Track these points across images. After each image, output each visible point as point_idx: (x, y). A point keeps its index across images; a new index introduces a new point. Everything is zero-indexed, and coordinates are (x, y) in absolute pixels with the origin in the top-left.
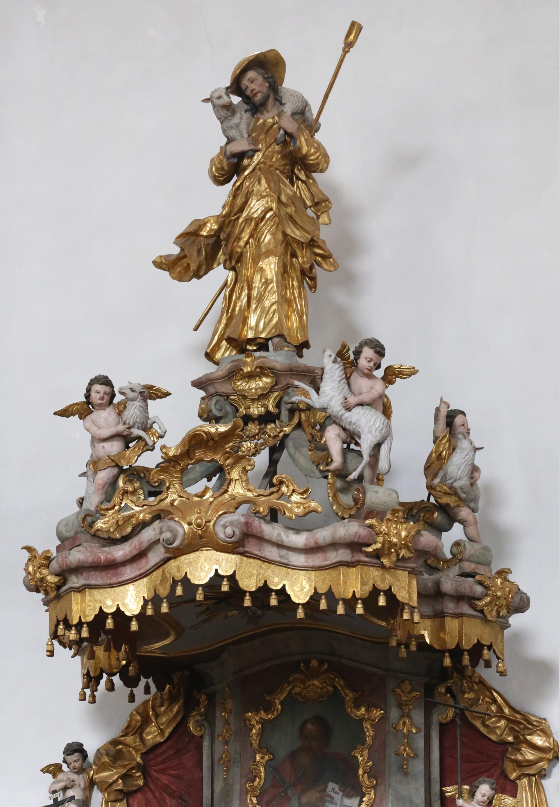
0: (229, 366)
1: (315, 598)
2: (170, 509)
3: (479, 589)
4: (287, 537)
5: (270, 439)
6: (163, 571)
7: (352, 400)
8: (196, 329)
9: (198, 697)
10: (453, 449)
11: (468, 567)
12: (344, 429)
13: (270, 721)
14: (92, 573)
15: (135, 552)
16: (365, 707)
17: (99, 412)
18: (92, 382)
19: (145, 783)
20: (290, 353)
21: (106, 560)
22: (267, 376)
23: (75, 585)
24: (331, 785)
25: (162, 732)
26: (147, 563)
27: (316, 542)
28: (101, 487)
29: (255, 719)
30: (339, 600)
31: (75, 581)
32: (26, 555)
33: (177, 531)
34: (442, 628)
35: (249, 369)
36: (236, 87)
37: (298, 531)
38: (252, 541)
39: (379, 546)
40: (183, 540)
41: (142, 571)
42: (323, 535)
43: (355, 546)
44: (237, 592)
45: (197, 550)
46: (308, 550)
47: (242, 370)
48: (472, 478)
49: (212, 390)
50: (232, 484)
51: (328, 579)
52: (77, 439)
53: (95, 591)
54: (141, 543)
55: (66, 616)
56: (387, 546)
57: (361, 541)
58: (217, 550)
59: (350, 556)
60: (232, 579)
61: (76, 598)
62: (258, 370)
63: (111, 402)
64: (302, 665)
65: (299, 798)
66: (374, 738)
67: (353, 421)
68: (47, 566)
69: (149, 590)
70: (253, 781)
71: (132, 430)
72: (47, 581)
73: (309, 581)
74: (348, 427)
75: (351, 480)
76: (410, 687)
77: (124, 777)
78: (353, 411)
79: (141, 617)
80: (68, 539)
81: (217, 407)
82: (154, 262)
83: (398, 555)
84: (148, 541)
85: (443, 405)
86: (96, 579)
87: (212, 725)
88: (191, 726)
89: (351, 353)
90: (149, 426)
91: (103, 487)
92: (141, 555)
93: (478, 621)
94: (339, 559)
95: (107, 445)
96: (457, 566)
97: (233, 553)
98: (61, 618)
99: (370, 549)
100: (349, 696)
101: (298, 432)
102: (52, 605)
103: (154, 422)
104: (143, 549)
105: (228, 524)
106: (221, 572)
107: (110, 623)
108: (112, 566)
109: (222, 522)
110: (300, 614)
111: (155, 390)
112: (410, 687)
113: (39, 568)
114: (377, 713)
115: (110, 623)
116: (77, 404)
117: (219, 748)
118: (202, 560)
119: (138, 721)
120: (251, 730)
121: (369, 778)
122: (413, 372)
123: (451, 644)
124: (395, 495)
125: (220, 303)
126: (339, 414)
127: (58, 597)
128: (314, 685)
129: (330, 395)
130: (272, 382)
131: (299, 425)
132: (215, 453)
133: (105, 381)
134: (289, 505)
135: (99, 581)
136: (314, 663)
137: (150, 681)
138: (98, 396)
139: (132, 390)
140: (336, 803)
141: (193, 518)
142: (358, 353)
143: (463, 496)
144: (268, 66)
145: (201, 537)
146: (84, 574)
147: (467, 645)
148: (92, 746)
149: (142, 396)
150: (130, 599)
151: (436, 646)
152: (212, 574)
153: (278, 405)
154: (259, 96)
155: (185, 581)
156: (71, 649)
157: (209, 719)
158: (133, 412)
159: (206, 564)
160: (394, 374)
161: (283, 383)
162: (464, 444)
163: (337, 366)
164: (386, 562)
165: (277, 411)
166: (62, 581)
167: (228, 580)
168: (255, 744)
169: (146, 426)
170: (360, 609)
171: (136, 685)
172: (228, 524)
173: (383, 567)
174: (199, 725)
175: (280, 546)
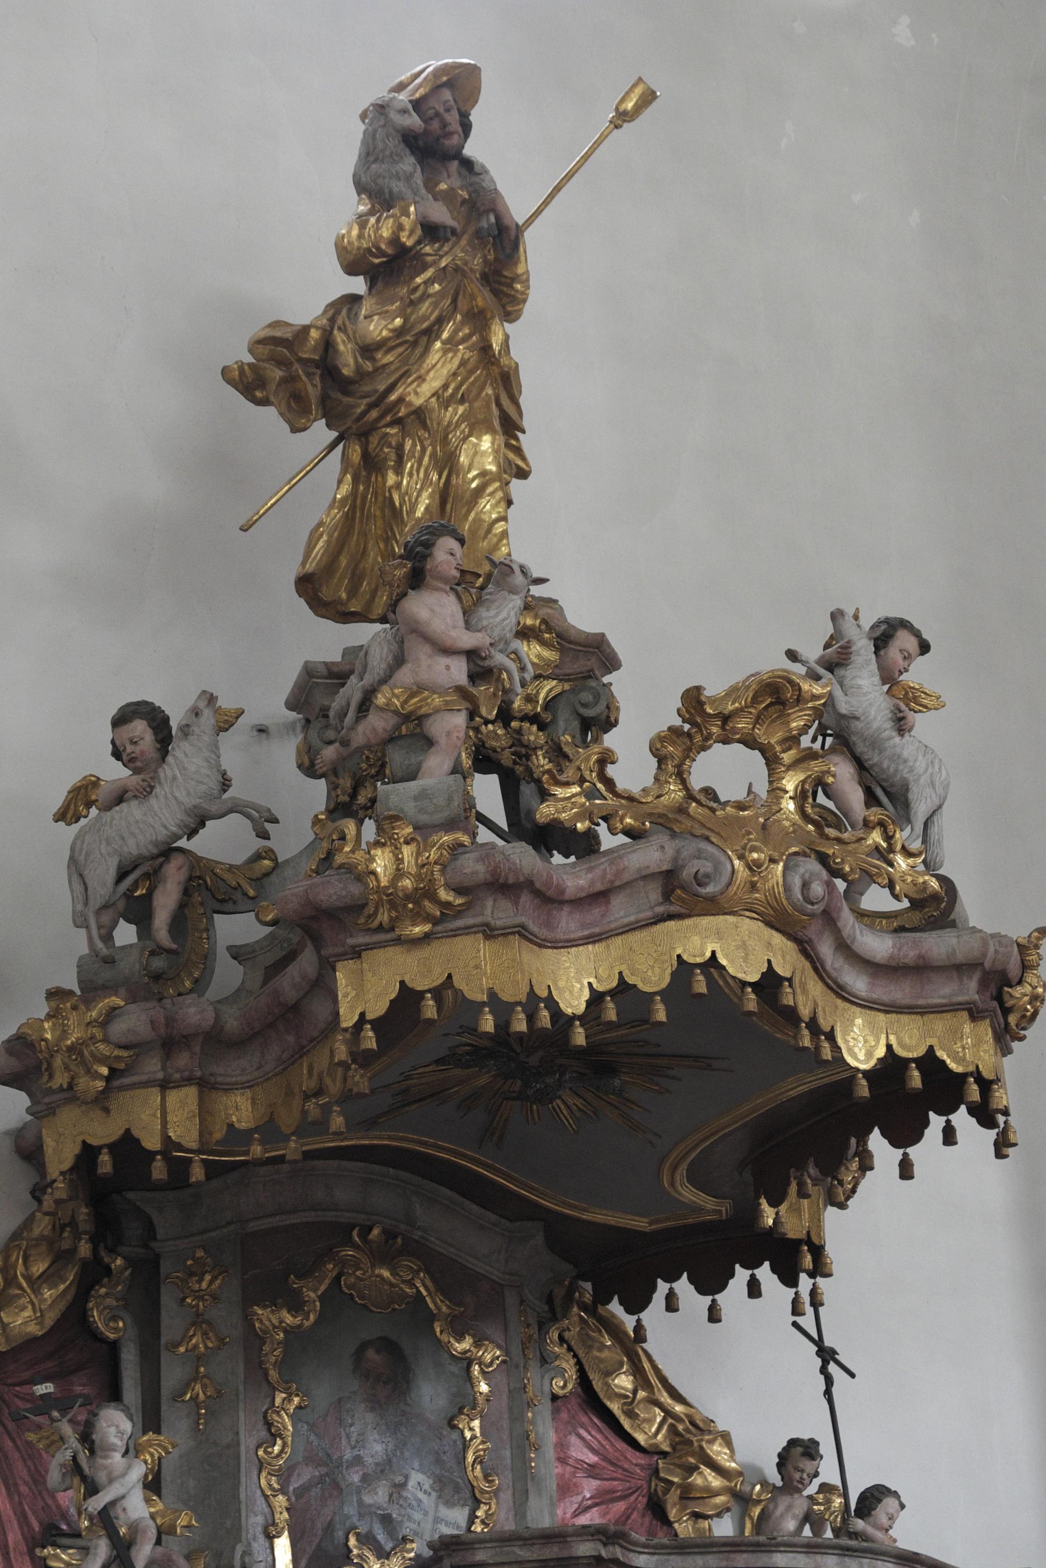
4: (862, 935)
9: (107, 1260)
16: (473, 1336)
25: (40, 1320)
26: (603, 916)
84: (639, 870)
110: (863, 1089)
168: (273, 1375)
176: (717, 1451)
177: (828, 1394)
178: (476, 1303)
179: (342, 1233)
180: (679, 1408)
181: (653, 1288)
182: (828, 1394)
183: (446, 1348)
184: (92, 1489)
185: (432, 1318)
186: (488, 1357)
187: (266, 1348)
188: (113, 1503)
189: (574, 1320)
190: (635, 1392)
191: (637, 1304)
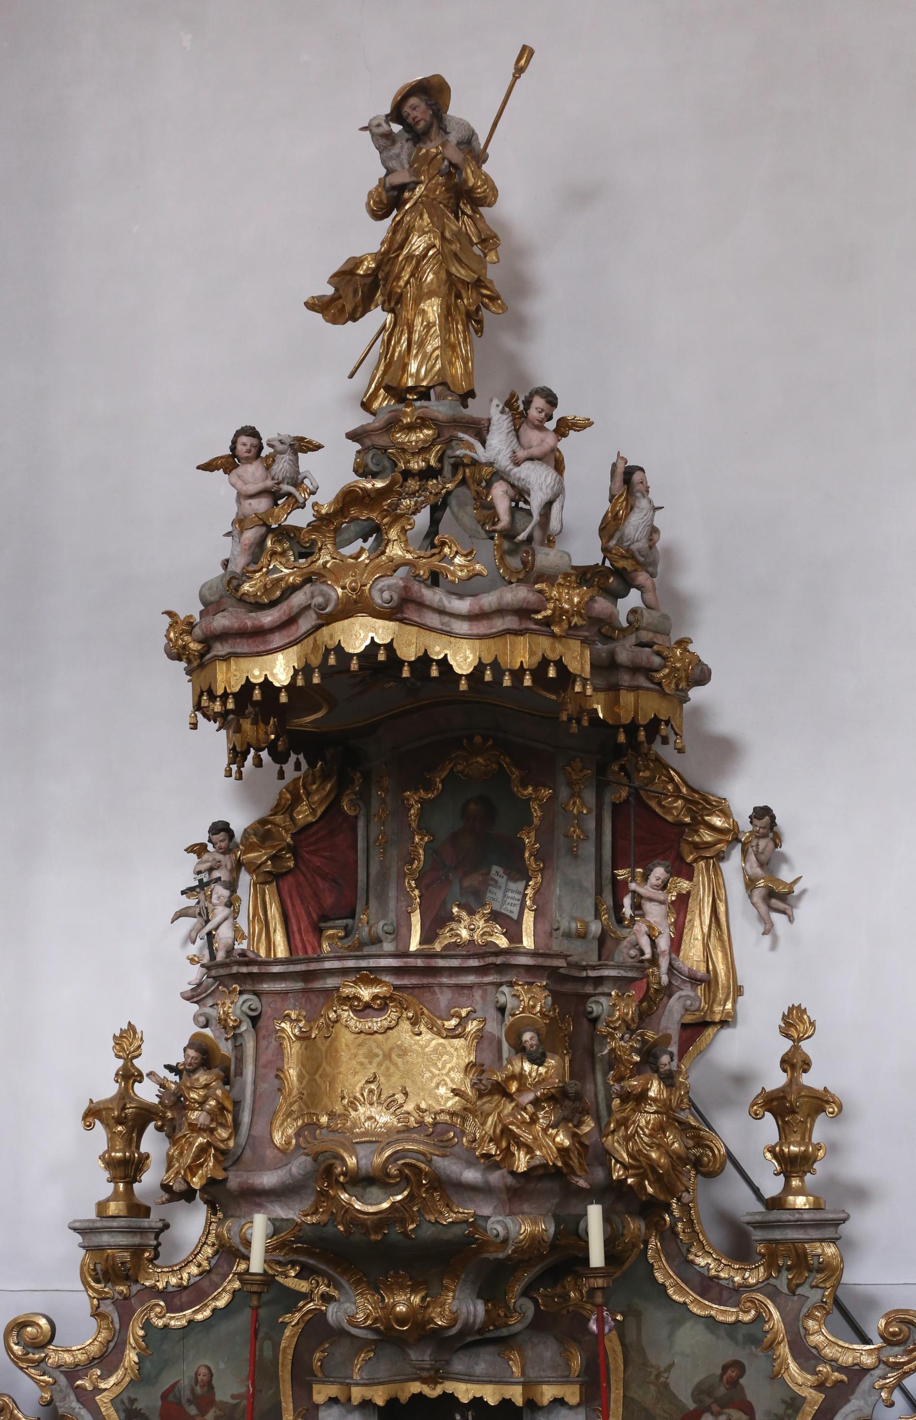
0: (387, 417)
1: (480, 668)
2: (323, 572)
3: (657, 660)
4: (450, 602)
5: (432, 496)
6: (315, 638)
7: (522, 454)
8: (351, 376)
10: (630, 508)
11: (646, 636)
12: (513, 486)
13: (429, 800)
14: (238, 640)
15: (284, 618)
16: (532, 786)
17: (245, 466)
18: (238, 434)
19: (296, 865)
20: (454, 403)
21: (253, 626)
22: (429, 428)
23: (220, 653)
24: (495, 868)
25: (314, 811)
27: (481, 609)
28: (247, 547)
29: (414, 800)
30: (505, 671)
31: (220, 649)
32: (167, 620)
33: (330, 595)
34: (616, 701)
35: (409, 420)
36: (397, 114)
37: (461, 596)
38: (412, 607)
39: (549, 612)
40: (337, 605)
41: (292, 638)
42: (489, 600)
43: (523, 612)
44: (394, 661)
45: (352, 616)
46: (471, 617)
47: (401, 421)
48: (651, 540)
49: (368, 442)
50: (390, 545)
51: (493, 648)
52: (221, 495)
53: (241, 660)
54: (291, 608)
55: (210, 687)
56: (557, 613)
57: (530, 607)
58: (373, 617)
59: (518, 624)
60: (389, 647)
61: (221, 667)
62: (419, 421)
63: (258, 455)
64: (465, 741)
65: (461, 882)
66: (542, 819)
67: (522, 477)
68: (190, 633)
69: (299, 659)
70: (412, 864)
71: (281, 486)
72: (190, 649)
73: (473, 651)
74: (516, 483)
75: (520, 540)
76: (580, 765)
77: (273, 858)
78: (523, 465)
79: (291, 687)
80: (212, 603)
81: (374, 461)
82: (306, 304)
83: (570, 623)
84: (299, 606)
85: (620, 461)
86: (243, 646)
87: (368, 805)
89: (520, 402)
90: (299, 481)
91: (250, 547)
92: (291, 621)
93: (655, 694)
94: (505, 627)
95: (254, 502)
96: (634, 636)
97: (390, 619)
98: (205, 688)
99: (539, 617)
100: (515, 774)
101: (462, 490)
102: (195, 674)
103: (305, 477)
104: (293, 615)
105: (385, 588)
106: (377, 640)
107: (257, 694)
108: (260, 633)
109: (379, 586)
110: (463, 685)
111: (307, 442)
112: (580, 765)
113: (181, 634)
114: (546, 793)
115: (257, 694)
116: (222, 457)
117: (375, 830)
118: (357, 627)
119: (288, 800)
120: (410, 810)
121: (536, 861)
122: (588, 424)
123: (626, 719)
124: (567, 558)
125: (378, 348)
126: (508, 469)
127: (202, 666)
128: (477, 762)
129: (497, 449)
130: (434, 434)
131: (463, 482)
132: (372, 510)
133: (251, 432)
134: (452, 568)
135: (246, 649)
136: (478, 739)
137: (301, 757)
138: (244, 449)
139: (281, 442)
140: (500, 887)
141: (348, 581)
142: (528, 403)
143: (642, 559)
144: (431, 92)
145: (356, 602)
146: (230, 641)
147: (642, 720)
148: (239, 825)
149: (292, 449)
150: (280, 669)
151: (610, 721)
152: (368, 642)
153: (440, 460)
154: (422, 124)
155: (339, 649)
156: (215, 722)
157: (364, 798)
158: (282, 466)
159: (361, 632)
160: (567, 426)
161: (447, 435)
162: (643, 503)
163: (505, 417)
164: (556, 630)
165: (439, 466)
166: (206, 649)
167: (385, 649)
168: (414, 825)
169: (296, 482)
170: (528, 681)
171: (286, 762)
172: (385, 588)
173: (553, 635)
174: (353, 803)
175: (442, 612)
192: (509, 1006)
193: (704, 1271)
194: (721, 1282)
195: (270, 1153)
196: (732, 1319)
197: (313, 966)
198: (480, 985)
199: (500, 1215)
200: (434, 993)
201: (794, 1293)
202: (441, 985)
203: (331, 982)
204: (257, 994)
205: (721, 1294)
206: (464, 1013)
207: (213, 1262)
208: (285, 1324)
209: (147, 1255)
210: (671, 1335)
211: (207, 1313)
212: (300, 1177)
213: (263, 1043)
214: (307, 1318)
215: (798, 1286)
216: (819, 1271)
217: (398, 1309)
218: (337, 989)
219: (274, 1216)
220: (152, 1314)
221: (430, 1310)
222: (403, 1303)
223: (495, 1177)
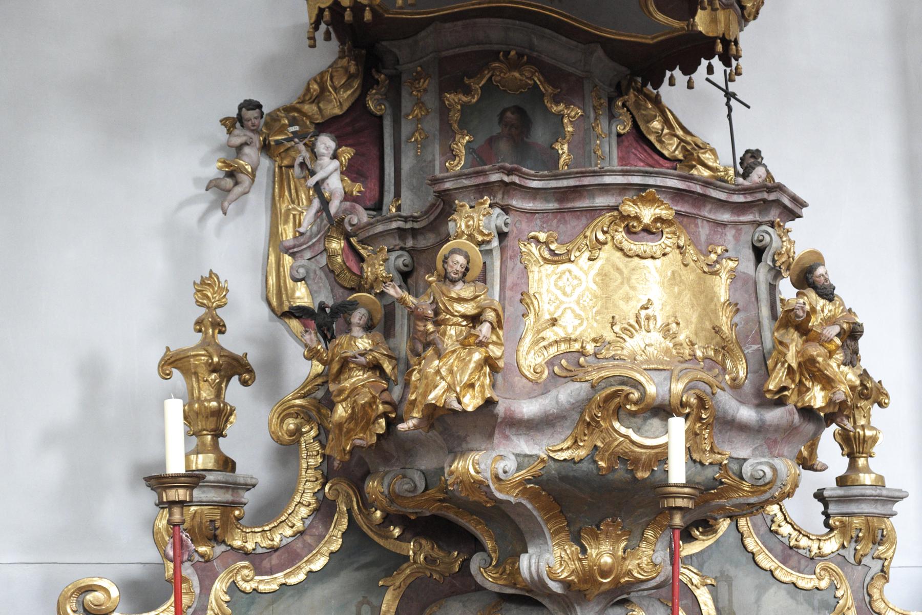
9: (376, 77)
70: (454, 160)
88: (371, 105)
119: (315, 90)
120: (449, 110)
151: (711, 35)
168: (456, 126)
176: (707, 157)
177: (729, 116)
178: (568, 86)
179: (494, 55)
180: (689, 139)
181: (664, 75)
182: (729, 116)
183: (547, 110)
184: (312, 173)
185: (543, 95)
186: (573, 114)
187: (451, 114)
188: (324, 180)
189: (631, 97)
190: (662, 130)
191: (657, 85)
192: (774, 245)
193: (785, 540)
194: (800, 551)
195: (519, 382)
196: (809, 585)
197: (586, 181)
198: (735, 224)
199: (764, 456)
200: (696, 225)
201: (859, 563)
202: (704, 218)
203: (601, 201)
204: (506, 209)
205: (799, 562)
206: (719, 250)
207: (308, 522)
208: (386, 588)
209: (237, 513)
210: (758, 600)
211: (301, 576)
212: (568, 406)
213: (510, 264)
214: (409, 581)
215: (866, 555)
216: (880, 543)
217: (602, 561)
218: (615, 208)
219: (518, 451)
220: (239, 578)
221: (627, 562)
222: (603, 553)
223: (774, 415)
